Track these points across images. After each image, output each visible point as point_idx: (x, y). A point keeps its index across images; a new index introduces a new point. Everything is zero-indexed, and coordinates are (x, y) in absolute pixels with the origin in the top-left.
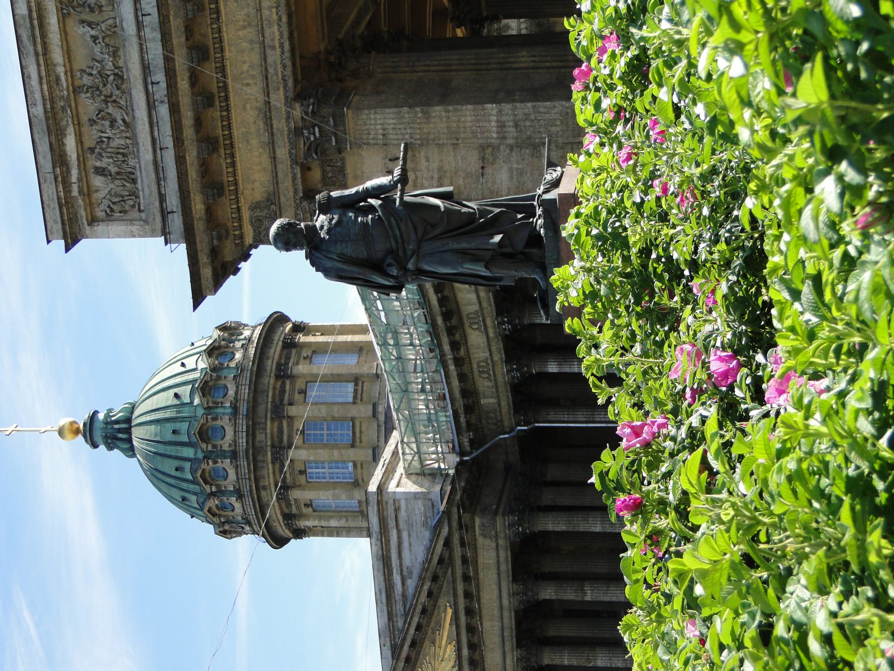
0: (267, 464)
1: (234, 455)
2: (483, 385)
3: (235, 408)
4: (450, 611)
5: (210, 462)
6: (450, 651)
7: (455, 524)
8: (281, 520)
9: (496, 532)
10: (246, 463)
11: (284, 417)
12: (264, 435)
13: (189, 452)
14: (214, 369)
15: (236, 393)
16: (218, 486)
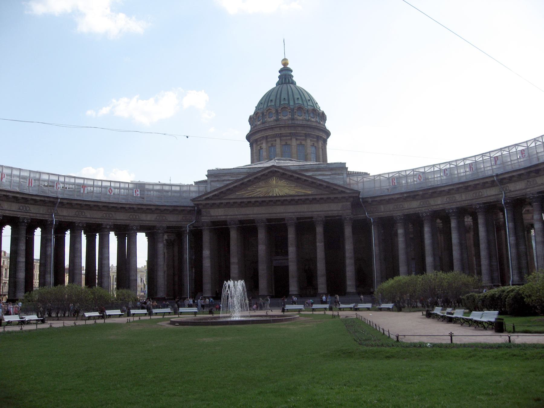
0: (290, 131)
1: (293, 119)
2: (391, 207)
3: (309, 120)
4: (310, 192)
5: (289, 111)
6: (292, 193)
7: (350, 195)
8: (265, 135)
9: (345, 210)
10: (290, 123)
11: (306, 137)
12: (300, 130)
13: (292, 103)
14: (319, 114)
15: (313, 121)
16: (280, 113)
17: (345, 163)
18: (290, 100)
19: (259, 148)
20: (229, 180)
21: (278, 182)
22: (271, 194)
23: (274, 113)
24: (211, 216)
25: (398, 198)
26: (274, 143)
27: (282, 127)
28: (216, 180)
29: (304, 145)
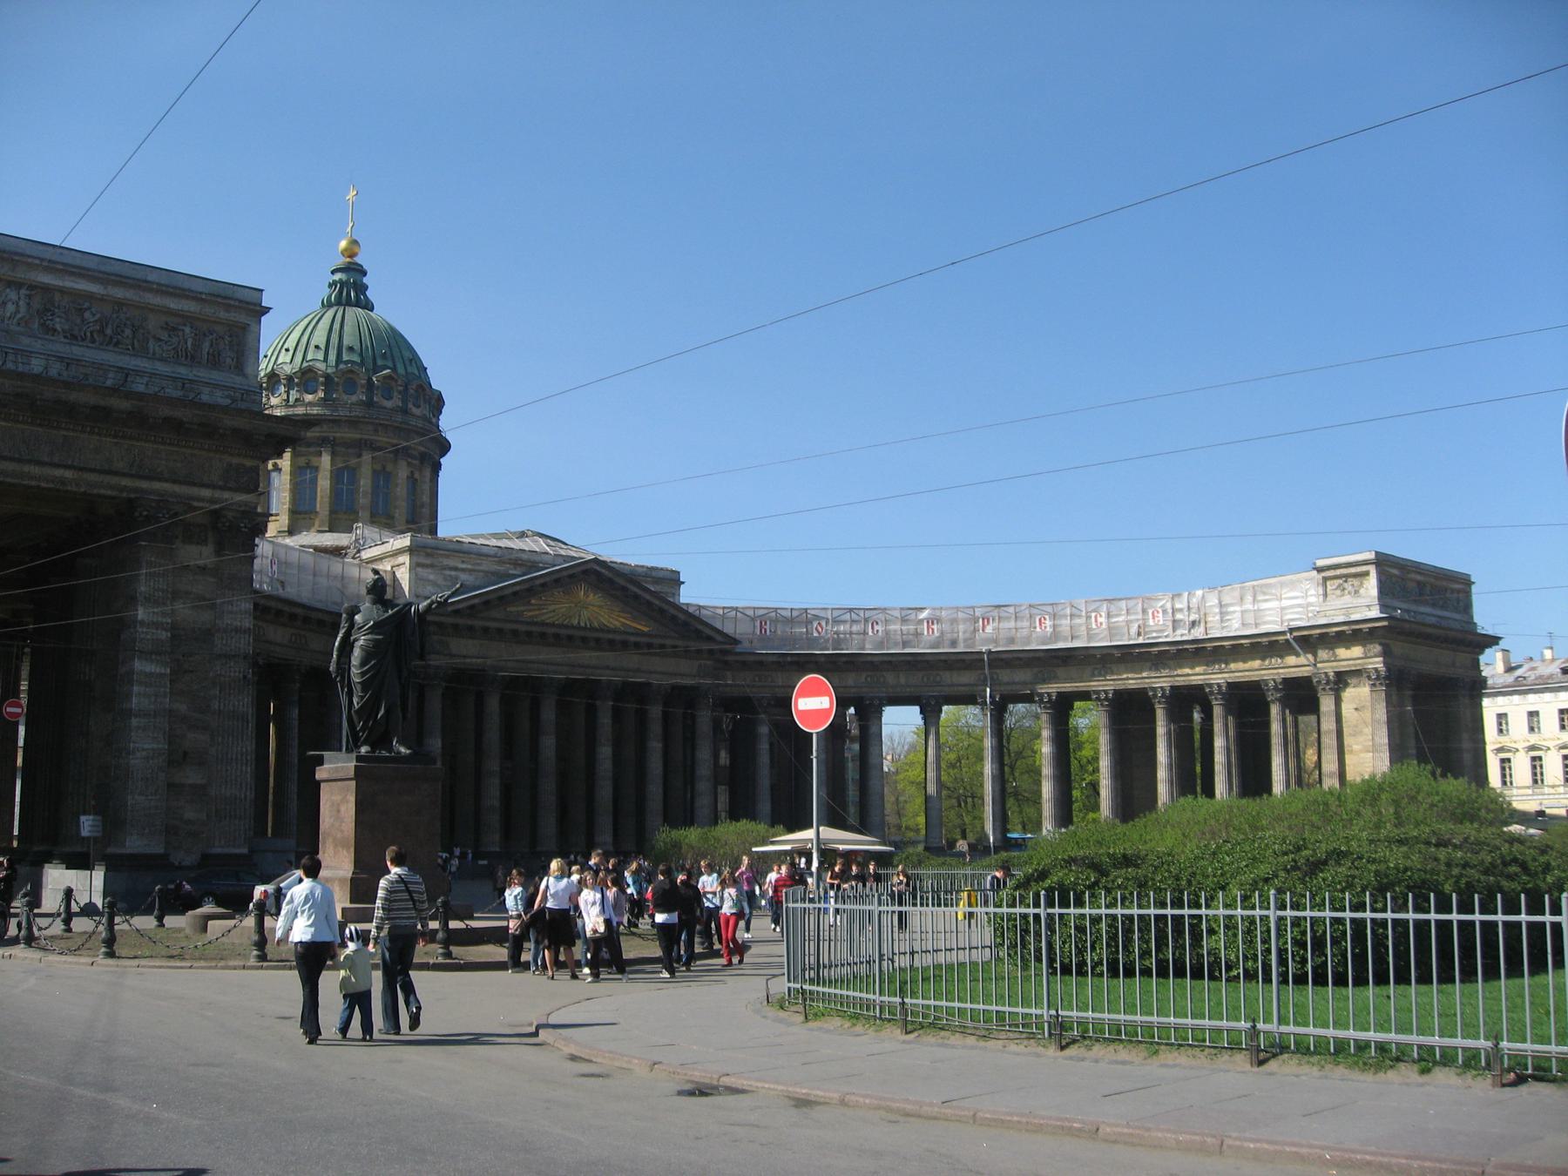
3: (431, 423)
4: (646, 629)
8: (334, 434)
11: (422, 463)
13: (401, 370)
17: (679, 573)
18: (397, 360)
19: (305, 465)
20: (456, 569)
21: (588, 596)
22: (575, 622)
23: (362, 386)
24: (452, 656)
25: (773, 662)
26: (353, 461)
27: (381, 424)
28: (428, 561)
29: (416, 480)
